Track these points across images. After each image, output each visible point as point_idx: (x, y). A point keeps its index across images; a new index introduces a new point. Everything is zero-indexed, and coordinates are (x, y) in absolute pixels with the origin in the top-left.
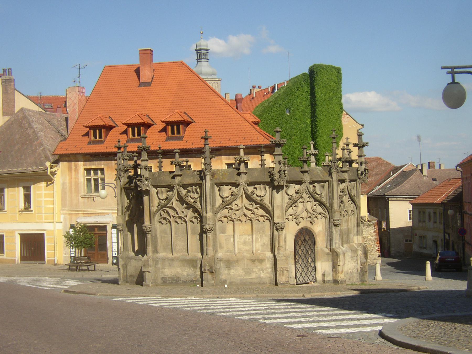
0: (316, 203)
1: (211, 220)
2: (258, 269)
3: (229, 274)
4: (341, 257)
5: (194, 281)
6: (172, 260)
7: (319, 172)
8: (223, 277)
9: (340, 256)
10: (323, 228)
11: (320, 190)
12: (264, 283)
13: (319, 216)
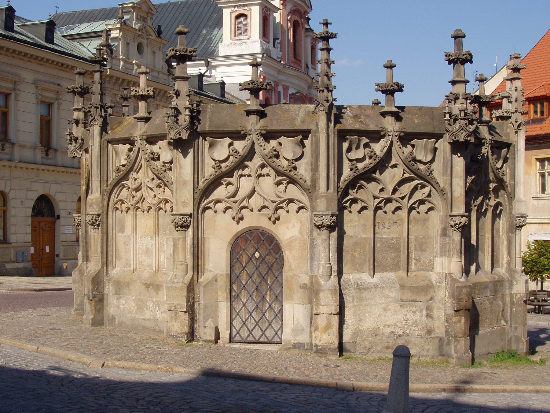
0: (279, 178)
1: (95, 206)
2: (153, 302)
3: (118, 306)
9: (321, 295)
10: (301, 232)
11: (294, 152)
12: (160, 332)
13: (293, 207)
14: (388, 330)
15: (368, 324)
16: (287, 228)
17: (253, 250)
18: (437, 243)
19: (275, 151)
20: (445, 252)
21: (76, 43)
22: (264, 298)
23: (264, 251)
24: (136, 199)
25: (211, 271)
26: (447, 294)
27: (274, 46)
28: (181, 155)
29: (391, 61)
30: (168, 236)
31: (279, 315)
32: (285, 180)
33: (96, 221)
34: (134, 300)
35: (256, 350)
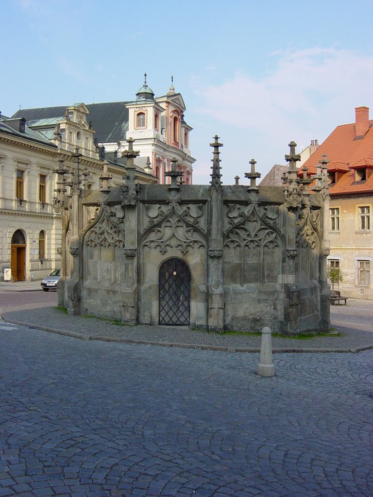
2: (112, 301)
9: (214, 297)
10: (201, 260)
11: (197, 213)
13: (196, 245)
15: (240, 313)
19: (186, 212)
21: (37, 132)
22: (178, 299)
24: (101, 239)
27: (162, 133)
29: (253, 160)
33: (76, 252)
35: (175, 329)
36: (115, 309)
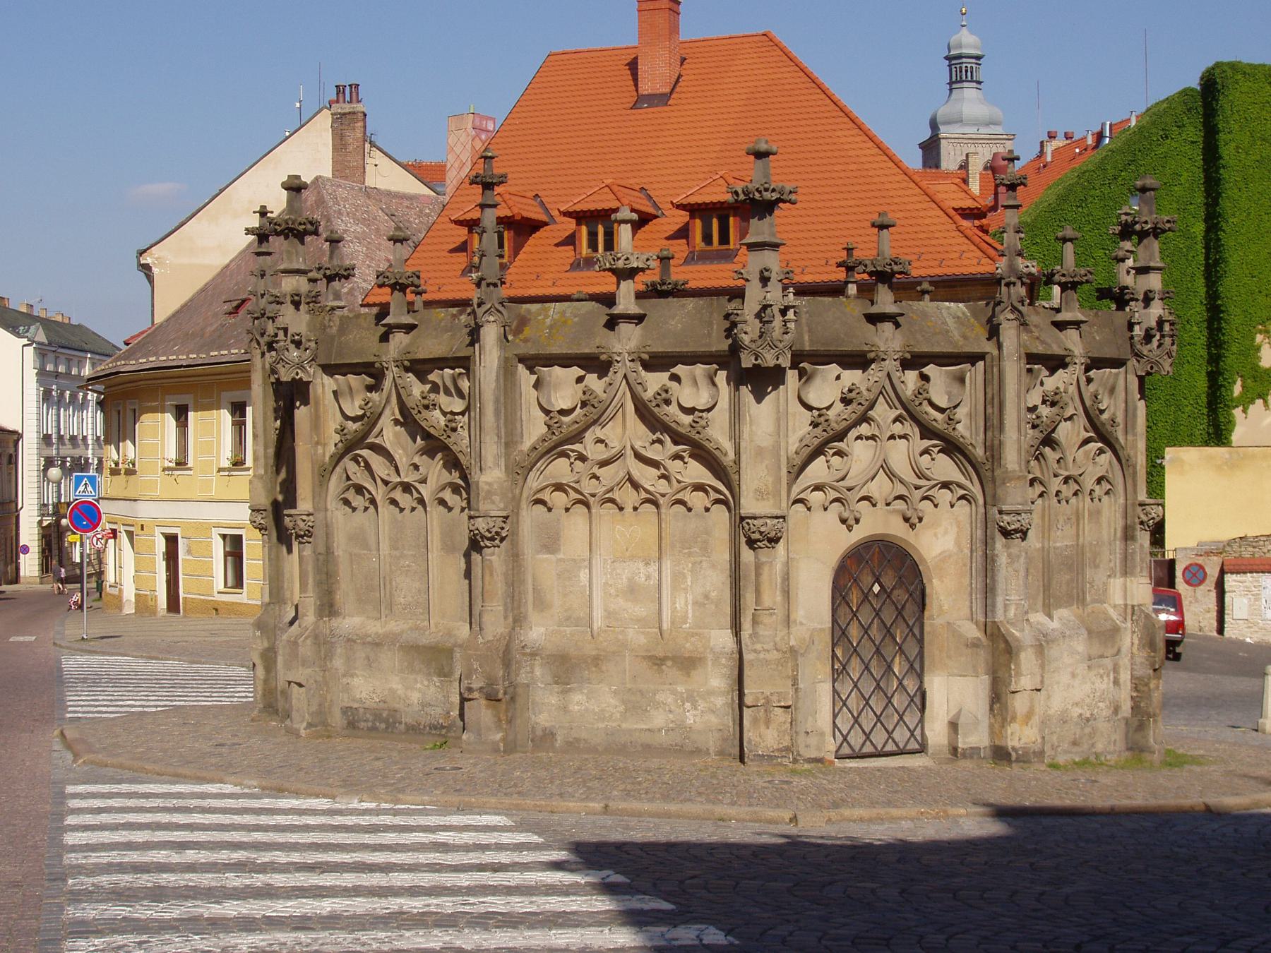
0: (927, 443)
1: (496, 498)
2: (674, 693)
3: (565, 709)
4: (1027, 659)
5: (443, 727)
6: (377, 645)
7: (950, 322)
8: (543, 719)
9: (1023, 656)
10: (958, 543)
11: (949, 394)
12: (697, 752)
13: (944, 496)
14: (1076, 712)
16: (935, 535)
17: (870, 579)
18: (1112, 554)
20: (1127, 569)
23: (889, 581)
25: (801, 624)
26: (1136, 642)
28: (751, 398)
30: (699, 559)
31: (917, 700)
32: (935, 446)
34: (615, 692)
36: (691, 718)
